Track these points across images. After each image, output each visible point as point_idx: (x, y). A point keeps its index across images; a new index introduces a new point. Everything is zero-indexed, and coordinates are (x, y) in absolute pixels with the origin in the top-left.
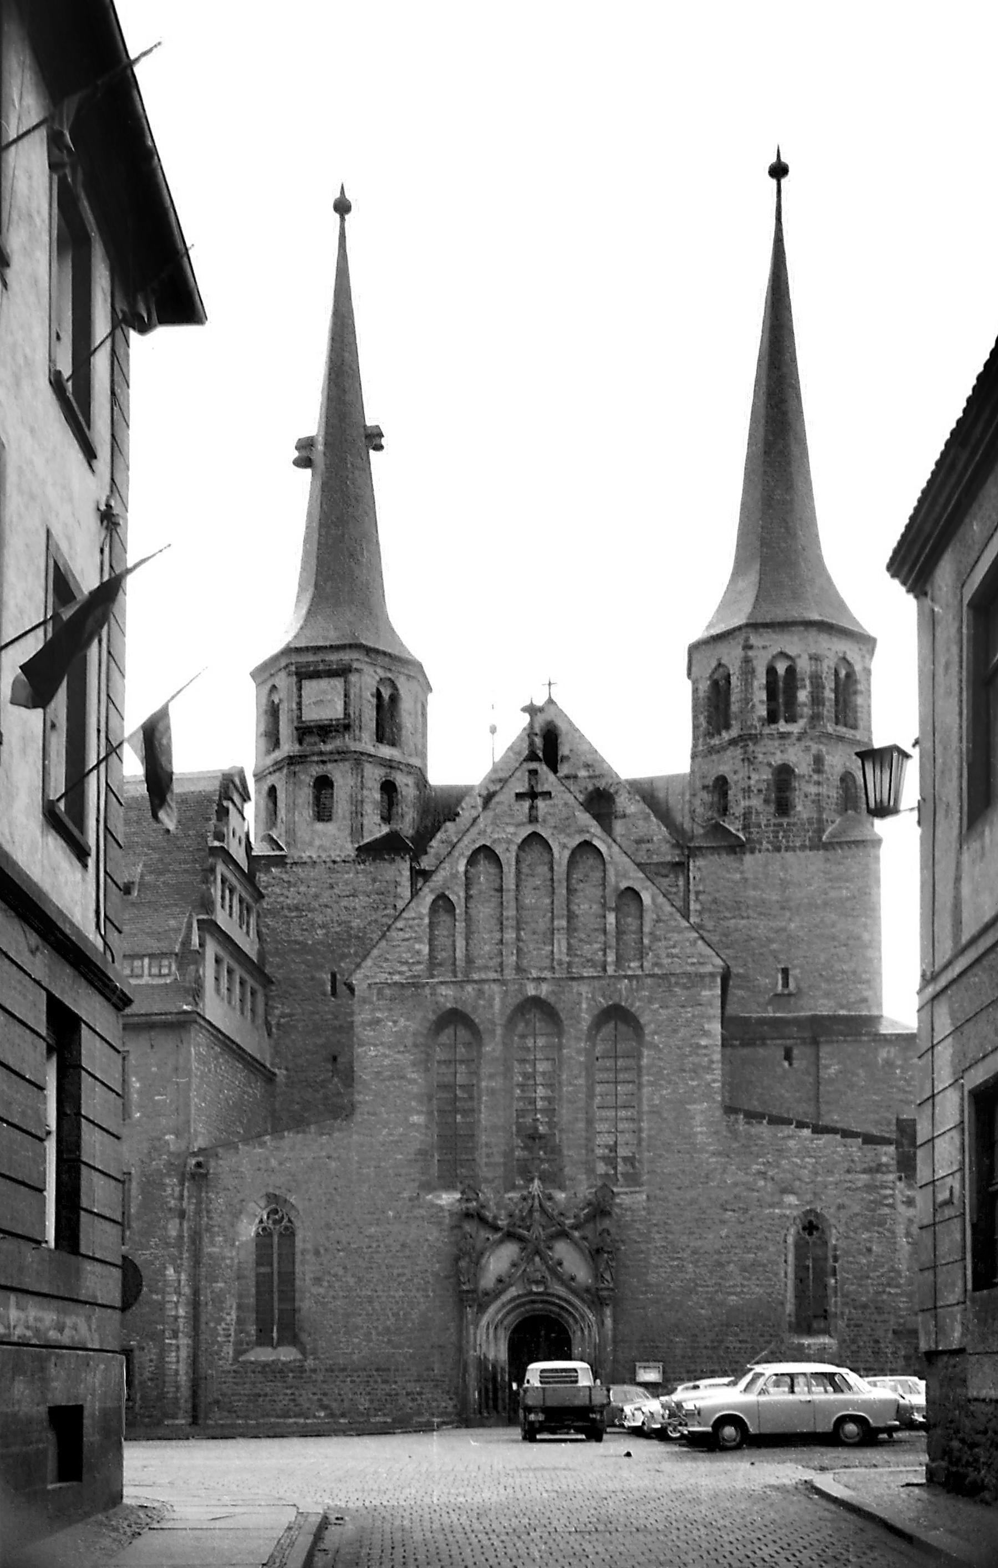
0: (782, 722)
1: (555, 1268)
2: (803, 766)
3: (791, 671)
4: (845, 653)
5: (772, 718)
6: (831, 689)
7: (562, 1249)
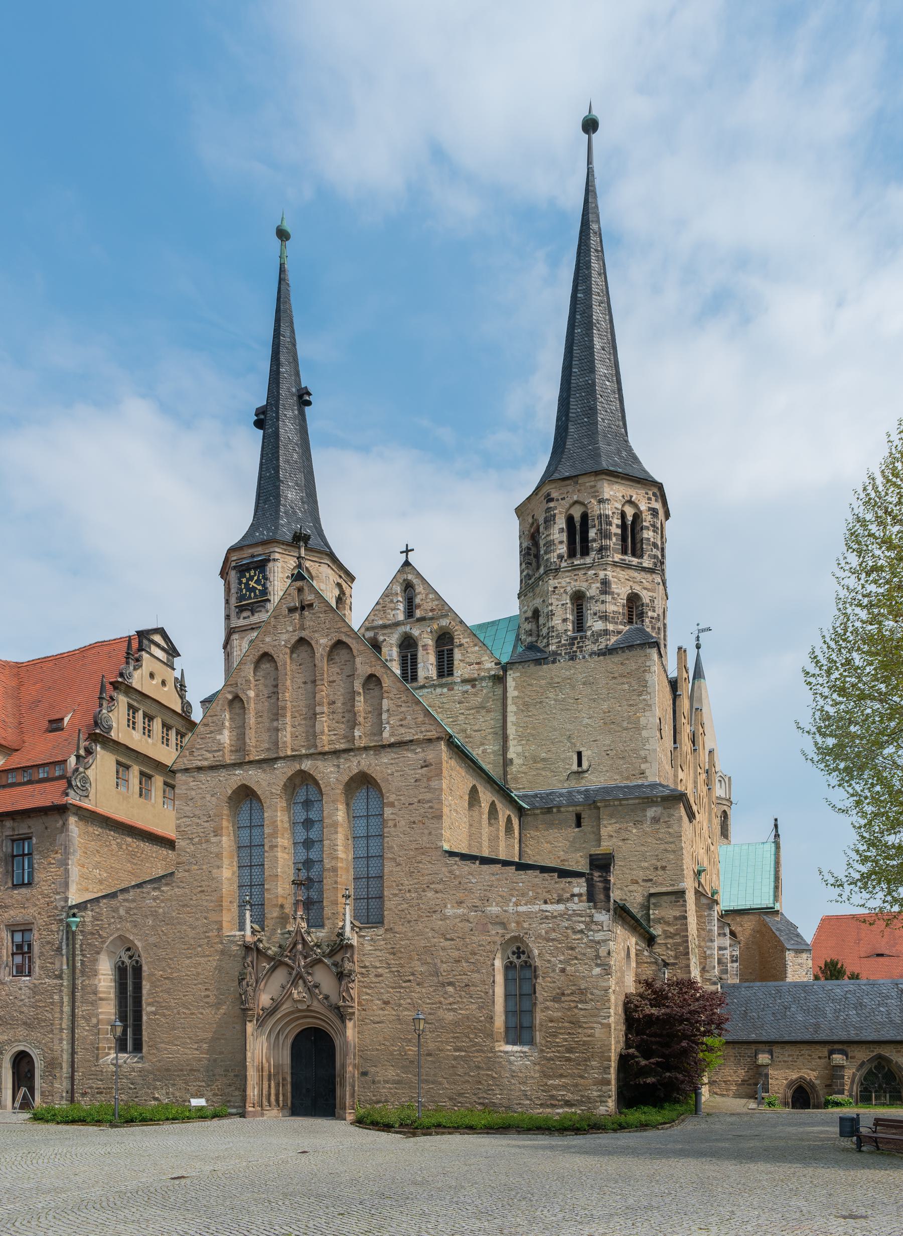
6: (617, 526)
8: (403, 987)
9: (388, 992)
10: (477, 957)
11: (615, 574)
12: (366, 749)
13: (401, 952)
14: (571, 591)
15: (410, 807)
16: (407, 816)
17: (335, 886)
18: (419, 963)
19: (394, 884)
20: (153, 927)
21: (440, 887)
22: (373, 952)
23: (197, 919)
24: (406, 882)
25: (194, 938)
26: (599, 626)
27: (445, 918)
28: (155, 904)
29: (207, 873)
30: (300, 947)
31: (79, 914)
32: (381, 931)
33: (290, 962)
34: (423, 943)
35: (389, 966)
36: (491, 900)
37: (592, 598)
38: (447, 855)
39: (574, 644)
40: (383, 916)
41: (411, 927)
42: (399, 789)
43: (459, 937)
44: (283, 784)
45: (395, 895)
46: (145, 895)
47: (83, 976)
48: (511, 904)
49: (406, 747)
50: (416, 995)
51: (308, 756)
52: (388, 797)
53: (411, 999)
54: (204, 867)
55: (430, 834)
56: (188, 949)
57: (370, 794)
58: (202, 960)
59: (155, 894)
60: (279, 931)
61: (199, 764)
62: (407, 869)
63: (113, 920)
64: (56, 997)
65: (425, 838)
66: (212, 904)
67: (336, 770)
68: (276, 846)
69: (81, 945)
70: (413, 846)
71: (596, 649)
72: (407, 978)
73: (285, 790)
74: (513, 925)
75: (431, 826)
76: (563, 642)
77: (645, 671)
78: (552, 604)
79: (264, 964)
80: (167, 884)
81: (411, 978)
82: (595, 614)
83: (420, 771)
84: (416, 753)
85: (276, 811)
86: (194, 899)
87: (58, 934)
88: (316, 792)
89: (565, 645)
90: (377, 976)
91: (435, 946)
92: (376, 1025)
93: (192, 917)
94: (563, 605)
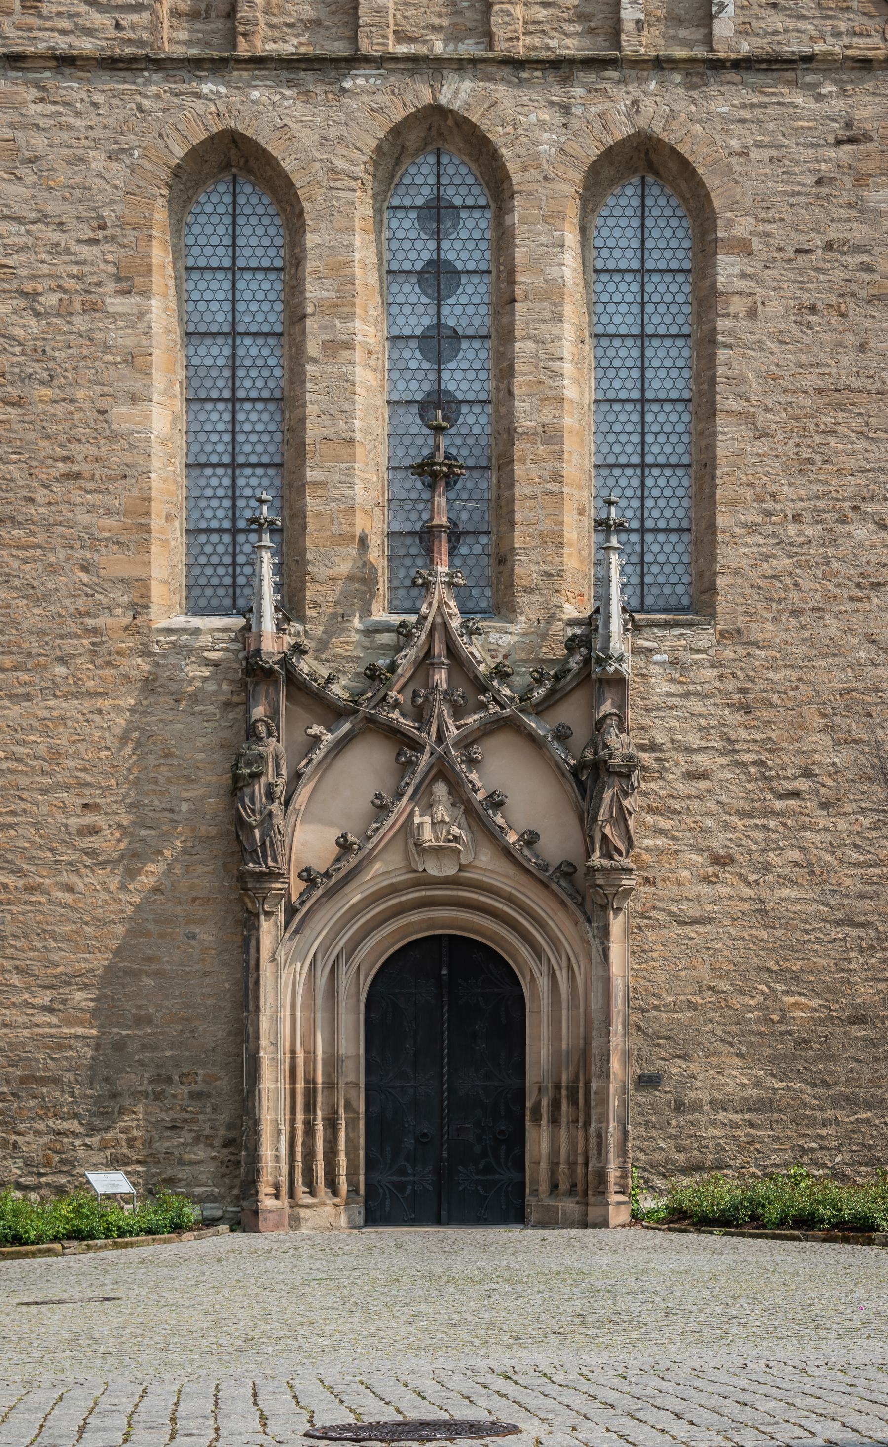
8: (775, 814)
9: (727, 827)
12: (660, 64)
13: (771, 705)
15: (801, 259)
16: (790, 288)
17: (553, 487)
18: (827, 740)
19: (749, 494)
22: (677, 701)
23: (53, 569)
24: (787, 489)
25: (42, 633)
29: (92, 415)
30: (441, 677)
32: (705, 637)
33: (407, 724)
34: (839, 680)
35: (730, 746)
40: (712, 589)
41: (803, 627)
42: (764, 202)
44: (374, 144)
45: (753, 528)
49: (790, 75)
50: (817, 839)
51: (462, 65)
52: (729, 224)
53: (802, 849)
54: (80, 394)
55: (863, 347)
57: (649, 202)
60: (357, 623)
62: (791, 450)
65: (846, 360)
67: (558, 119)
68: (349, 346)
70: (811, 381)
72: (788, 785)
73: (376, 164)
75: (868, 323)
79: (316, 730)
81: (802, 784)
83: (831, 153)
84: (820, 97)
85: (349, 230)
86: (40, 500)
88: (470, 180)
90: (690, 776)
91: (877, 690)
92: (689, 930)
93: (36, 559)
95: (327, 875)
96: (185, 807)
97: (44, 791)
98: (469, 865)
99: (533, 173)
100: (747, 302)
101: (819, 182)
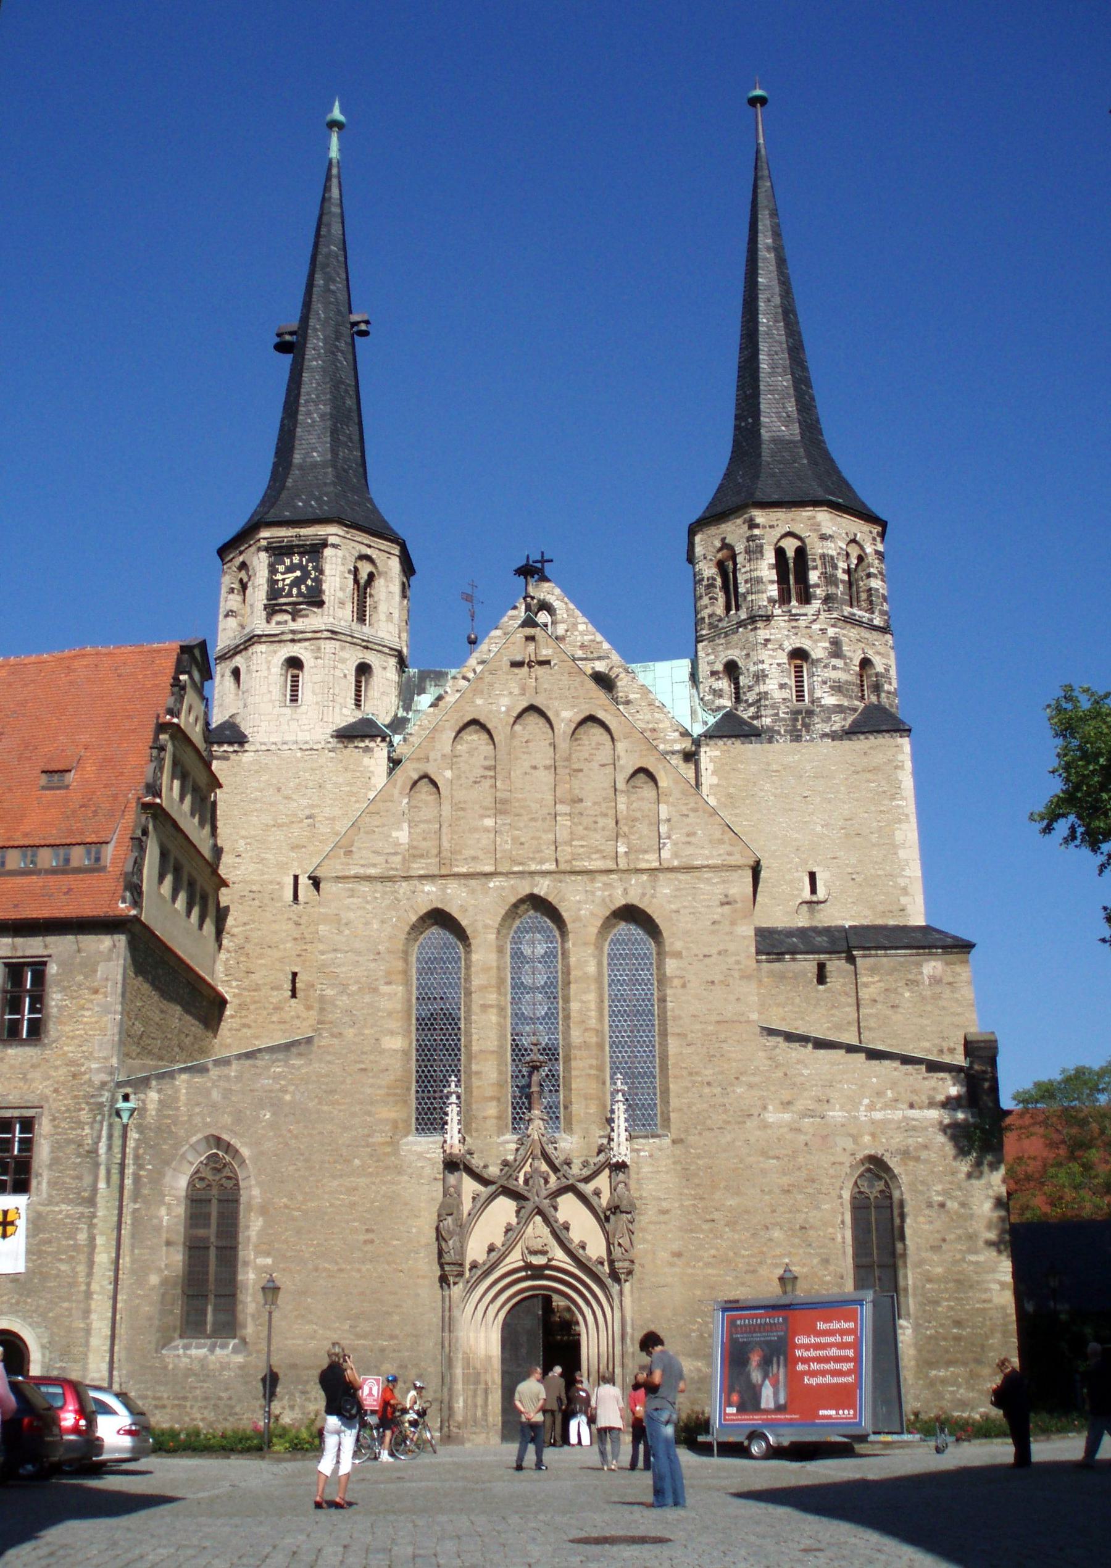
0: (794, 603)
1: (559, 1235)
2: (818, 651)
3: (801, 552)
4: (855, 535)
5: (784, 598)
7: (569, 1209)
10: (815, 1185)
11: (844, 632)
14: (790, 648)
19: (685, 1073)
20: (272, 1125)
21: (756, 1079)
23: (353, 1115)
26: (830, 700)
27: (765, 1126)
28: (278, 1086)
31: (132, 1097)
32: (667, 1141)
36: (832, 1101)
37: (819, 660)
38: (765, 1033)
39: (796, 720)
42: (687, 932)
43: (787, 1155)
45: (687, 1089)
46: (258, 1071)
47: (135, 1201)
48: (862, 1108)
56: (335, 1162)
58: (362, 1181)
59: (278, 1070)
61: (362, 871)
63: (197, 1110)
64: (82, 1237)
66: (379, 1092)
69: (137, 1148)
70: (714, 1018)
71: (827, 730)
74: (867, 1139)
76: (782, 715)
77: (896, 768)
78: (763, 662)
80: (300, 1055)
82: (825, 683)
83: (719, 910)
87: (92, 1128)
89: (784, 719)
94: (779, 665)
95: (484, 1264)
96: (414, 1230)
97: (347, 1222)
98: (553, 1259)
99: (578, 924)
100: (681, 981)
101: (714, 923)
